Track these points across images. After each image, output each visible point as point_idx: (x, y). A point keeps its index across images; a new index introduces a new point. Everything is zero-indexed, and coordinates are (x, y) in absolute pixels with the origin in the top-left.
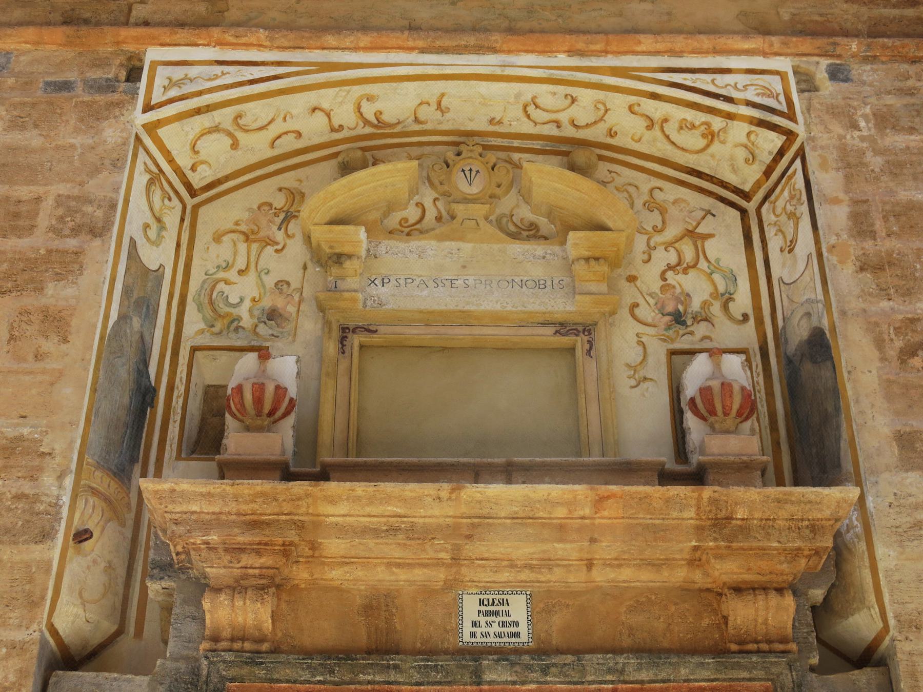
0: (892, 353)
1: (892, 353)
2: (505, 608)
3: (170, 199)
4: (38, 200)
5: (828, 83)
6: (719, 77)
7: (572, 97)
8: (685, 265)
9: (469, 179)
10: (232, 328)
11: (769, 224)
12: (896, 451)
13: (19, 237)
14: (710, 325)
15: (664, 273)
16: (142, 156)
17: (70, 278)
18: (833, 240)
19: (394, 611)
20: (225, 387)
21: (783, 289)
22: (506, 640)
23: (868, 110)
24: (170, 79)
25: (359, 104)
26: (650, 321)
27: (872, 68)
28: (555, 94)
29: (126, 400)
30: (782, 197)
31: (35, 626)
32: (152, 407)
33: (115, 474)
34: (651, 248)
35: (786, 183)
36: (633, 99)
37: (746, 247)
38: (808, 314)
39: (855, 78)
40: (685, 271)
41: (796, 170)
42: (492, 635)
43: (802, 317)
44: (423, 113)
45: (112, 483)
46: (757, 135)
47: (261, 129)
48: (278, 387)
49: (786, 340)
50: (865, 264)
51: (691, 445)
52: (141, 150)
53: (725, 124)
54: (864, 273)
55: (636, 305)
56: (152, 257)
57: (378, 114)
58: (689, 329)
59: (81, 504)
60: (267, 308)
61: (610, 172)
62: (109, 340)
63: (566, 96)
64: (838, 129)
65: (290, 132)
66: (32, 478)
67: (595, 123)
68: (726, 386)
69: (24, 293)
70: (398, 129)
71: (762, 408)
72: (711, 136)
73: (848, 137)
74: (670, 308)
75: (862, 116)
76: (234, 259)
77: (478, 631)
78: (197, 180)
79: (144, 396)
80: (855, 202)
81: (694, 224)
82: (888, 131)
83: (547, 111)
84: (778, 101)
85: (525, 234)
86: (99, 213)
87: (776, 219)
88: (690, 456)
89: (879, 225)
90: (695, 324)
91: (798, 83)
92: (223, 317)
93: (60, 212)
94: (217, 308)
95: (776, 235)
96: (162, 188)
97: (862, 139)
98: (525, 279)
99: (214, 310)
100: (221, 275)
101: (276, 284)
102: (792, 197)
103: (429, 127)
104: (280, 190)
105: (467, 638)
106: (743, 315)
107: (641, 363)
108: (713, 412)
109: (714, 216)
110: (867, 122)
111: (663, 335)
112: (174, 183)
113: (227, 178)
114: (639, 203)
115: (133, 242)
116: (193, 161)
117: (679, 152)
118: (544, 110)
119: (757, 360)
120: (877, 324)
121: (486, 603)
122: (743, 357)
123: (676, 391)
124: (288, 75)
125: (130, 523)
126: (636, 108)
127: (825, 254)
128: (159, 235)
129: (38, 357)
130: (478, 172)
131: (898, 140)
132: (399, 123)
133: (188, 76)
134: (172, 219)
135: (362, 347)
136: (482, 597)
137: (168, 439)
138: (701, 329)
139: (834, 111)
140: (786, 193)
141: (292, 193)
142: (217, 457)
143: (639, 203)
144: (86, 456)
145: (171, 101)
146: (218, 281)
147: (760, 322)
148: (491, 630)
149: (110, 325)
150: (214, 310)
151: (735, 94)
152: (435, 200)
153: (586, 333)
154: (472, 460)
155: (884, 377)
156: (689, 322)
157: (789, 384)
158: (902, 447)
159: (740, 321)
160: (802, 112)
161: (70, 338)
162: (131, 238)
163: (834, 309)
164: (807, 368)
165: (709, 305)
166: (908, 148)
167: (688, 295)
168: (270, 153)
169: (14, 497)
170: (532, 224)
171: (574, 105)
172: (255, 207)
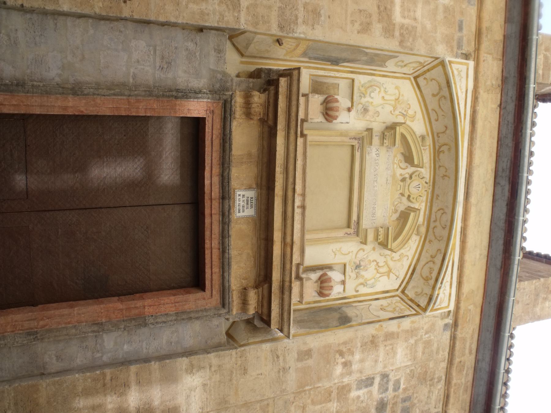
0: (341, 348)
2: (249, 207)
3: (413, 69)
6: (449, 283)
7: (445, 228)
8: (378, 269)
9: (417, 186)
11: (392, 300)
12: (304, 350)
13: (400, 12)
15: (376, 261)
16: (431, 60)
17: (383, 33)
18: (384, 326)
22: (238, 208)
23: (432, 337)
26: (358, 256)
27: (447, 339)
28: (447, 221)
30: (402, 306)
31: (246, 26)
32: (331, 64)
33: (305, 52)
34: (385, 256)
35: (407, 308)
37: (384, 291)
38: (357, 316)
39: (444, 333)
40: (376, 269)
41: (411, 311)
42: (239, 203)
43: (356, 314)
45: (301, 51)
46: (426, 297)
48: (337, 117)
49: (347, 307)
51: (310, 274)
52: (433, 59)
53: (431, 285)
54: (371, 337)
55: (364, 251)
58: (354, 271)
59: (294, 41)
60: (369, 108)
61: (415, 240)
62: (358, 49)
64: (426, 327)
65: (438, 117)
66: (304, 22)
67: (435, 236)
69: (378, 15)
70: (437, 159)
73: (423, 331)
74: (362, 263)
75: (430, 335)
76: (388, 95)
77: (241, 197)
80: (398, 334)
81: (394, 272)
82: (424, 345)
83: (440, 218)
85: (393, 208)
86: (409, 44)
87: (393, 303)
91: (444, 312)
92: (366, 91)
93: (410, 28)
96: (418, 67)
97: (421, 336)
98: (376, 209)
99: (368, 87)
101: (378, 112)
102: (401, 310)
103: (437, 171)
104: (415, 112)
105: (238, 193)
107: (341, 253)
109: (396, 279)
110: (427, 338)
111: (352, 261)
115: (397, 57)
119: (341, 296)
120: (352, 342)
121: (252, 200)
123: (329, 267)
124: (460, 118)
125: (285, 58)
126: (439, 252)
127: (379, 323)
128: (399, 66)
129: (353, 22)
130: (419, 190)
132: (439, 159)
133: (462, 79)
134: (405, 70)
135: (353, 146)
137: (318, 71)
138: (353, 275)
139: (433, 325)
140: (403, 307)
141: (414, 117)
145: (453, 72)
146: (380, 88)
147: (355, 296)
148: (241, 202)
149: (364, 50)
150: (368, 87)
151: (442, 290)
152: (408, 173)
155: (332, 345)
156: (356, 271)
158: (306, 351)
160: (433, 314)
161: (359, 34)
162: (398, 56)
164: (336, 315)
166: (417, 352)
167: (367, 270)
168: (430, 108)
171: (442, 228)
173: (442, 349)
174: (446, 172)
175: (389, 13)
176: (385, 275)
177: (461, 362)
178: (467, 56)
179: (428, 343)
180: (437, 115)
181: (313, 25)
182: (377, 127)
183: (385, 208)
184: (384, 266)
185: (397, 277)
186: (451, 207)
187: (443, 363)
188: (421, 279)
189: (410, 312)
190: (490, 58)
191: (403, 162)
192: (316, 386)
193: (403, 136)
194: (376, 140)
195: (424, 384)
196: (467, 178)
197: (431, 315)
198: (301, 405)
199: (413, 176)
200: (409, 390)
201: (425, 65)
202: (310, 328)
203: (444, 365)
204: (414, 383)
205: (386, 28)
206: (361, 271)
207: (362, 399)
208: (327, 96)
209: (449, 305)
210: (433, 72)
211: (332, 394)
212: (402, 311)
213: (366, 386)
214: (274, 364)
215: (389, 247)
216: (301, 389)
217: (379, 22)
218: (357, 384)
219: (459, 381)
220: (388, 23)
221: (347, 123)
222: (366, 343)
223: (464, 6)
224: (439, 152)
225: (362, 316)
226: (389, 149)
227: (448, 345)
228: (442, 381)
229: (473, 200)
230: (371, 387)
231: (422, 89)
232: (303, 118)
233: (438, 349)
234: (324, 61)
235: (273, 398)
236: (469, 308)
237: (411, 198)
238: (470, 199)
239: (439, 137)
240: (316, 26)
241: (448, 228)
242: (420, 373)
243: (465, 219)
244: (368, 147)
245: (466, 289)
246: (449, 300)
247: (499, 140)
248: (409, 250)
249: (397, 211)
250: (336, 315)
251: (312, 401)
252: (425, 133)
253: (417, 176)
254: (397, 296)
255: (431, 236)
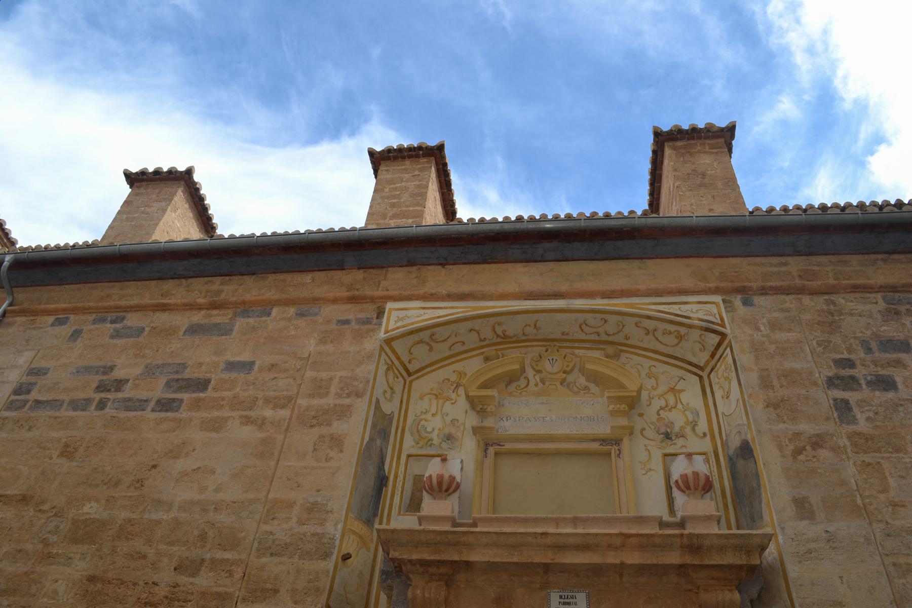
0: (788, 453)
1: (788, 452)
2: (574, 600)
3: (397, 378)
4: (331, 379)
5: (742, 307)
6: (682, 306)
7: (605, 320)
8: (670, 407)
10: (428, 444)
11: (715, 383)
12: (794, 510)
13: (321, 398)
14: (685, 439)
15: (658, 411)
16: (383, 356)
17: (345, 419)
19: (512, 601)
20: (424, 476)
21: (724, 418)
23: (765, 320)
24: (398, 317)
25: (494, 327)
28: (595, 318)
29: (372, 483)
30: (721, 369)
33: (364, 522)
34: (651, 398)
35: (723, 361)
36: (637, 319)
38: (739, 432)
39: (756, 304)
40: (670, 410)
41: (727, 354)
43: (736, 434)
44: (528, 330)
46: (705, 336)
47: (443, 341)
48: (451, 476)
49: (728, 447)
50: (769, 404)
52: (383, 353)
54: (769, 409)
55: (644, 429)
56: (388, 408)
57: (504, 332)
58: (674, 442)
59: (346, 538)
61: (627, 358)
63: (602, 319)
64: (749, 331)
66: (322, 524)
67: (618, 332)
68: (696, 474)
69: (322, 426)
70: (514, 339)
71: (716, 485)
72: (680, 337)
73: (755, 335)
74: (663, 430)
78: (412, 368)
79: (382, 481)
81: (674, 384)
82: (777, 331)
83: (592, 327)
84: (715, 318)
85: (582, 392)
86: (361, 386)
88: (676, 513)
89: (775, 382)
90: (677, 439)
94: (421, 435)
95: (719, 389)
96: (394, 372)
97: (763, 336)
98: (583, 416)
99: (420, 435)
100: (423, 416)
101: (451, 421)
102: (726, 369)
103: (531, 337)
106: (703, 434)
107: (648, 461)
108: (688, 488)
110: (765, 327)
112: (400, 369)
113: (427, 366)
114: (643, 374)
115: (378, 401)
116: (409, 358)
117: (664, 346)
118: (590, 327)
121: (563, 597)
122: (704, 456)
123: (668, 477)
125: (372, 549)
126: (639, 325)
127: (746, 399)
129: (328, 459)
130: (556, 360)
131: (782, 336)
132: (515, 336)
134: (398, 388)
135: (496, 454)
136: (561, 594)
138: (680, 442)
142: (418, 514)
143: (643, 374)
144: (350, 513)
145: (398, 328)
149: (365, 443)
150: (420, 435)
151: (692, 315)
152: (535, 375)
153: (617, 445)
154: (554, 516)
157: (731, 471)
159: (702, 437)
160: (729, 323)
161: (343, 450)
162: (377, 398)
163: (753, 430)
164: (741, 463)
165: (684, 429)
166: (788, 340)
167: (672, 423)
168: (448, 354)
169: (312, 535)
170: (586, 387)
172: (441, 381)
173: (782, 304)
174: (530, 326)
175: (321, 412)
176: (679, 396)
177: (800, 276)
178: (380, 313)
179: (774, 326)
180: (457, 343)
181: (327, 512)
182: (472, 420)
183: (582, 404)
184: (665, 399)
185: (682, 380)
186: (574, 315)
187: (803, 300)
188: (680, 345)
189: (728, 355)
190: (384, 284)
191: (518, 383)
192: (855, 488)
193: (484, 386)
194: (489, 422)
195: (840, 324)
196: (535, 298)
197: (731, 327)
198: (890, 509)
199: (537, 368)
200: (851, 344)
201: (390, 363)
202: (760, 502)
203: (806, 300)
204: (839, 338)
205: (338, 416)
206: (673, 431)
207: (871, 415)
208: (424, 491)
209: (714, 303)
210: (399, 351)
211: (867, 461)
212: (728, 367)
213: (850, 409)
214: (822, 557)
215: (635, 394)
216: (863, 511)
217: (331, 424)
218: (848, 424)
219: (831, 274)
220: (332, 413)
221: (462, 462)
222: (779, 416)
223: (321, 320)
224: (505, 337)
225: (739, 425)
226: (501, 404)
227: (775, 296)
228: (832, 298)
229: (564, 287)
230: (851, 402)
231: (424, 364)
232: (450, 524)
233: (782, 310)
234: (381, 495)
235: (881, 556)
236: (717, 274)
237: (568, 369)
238: (562, 291)
239: (485, 339)
240: (329, 508)
241: (604, 316)
242: (821, 331)
243: (590, 295)
244: (497, 431)
245: (689, 283)
246: (706, 303)
247: (485, 262)
248: (642, 366)
249: (586, 387)
250: (741, 463)
251: (881, 492)
252: (481, 357)
253: (537, 363)
254: (709, 376)
255: (619, 338)
